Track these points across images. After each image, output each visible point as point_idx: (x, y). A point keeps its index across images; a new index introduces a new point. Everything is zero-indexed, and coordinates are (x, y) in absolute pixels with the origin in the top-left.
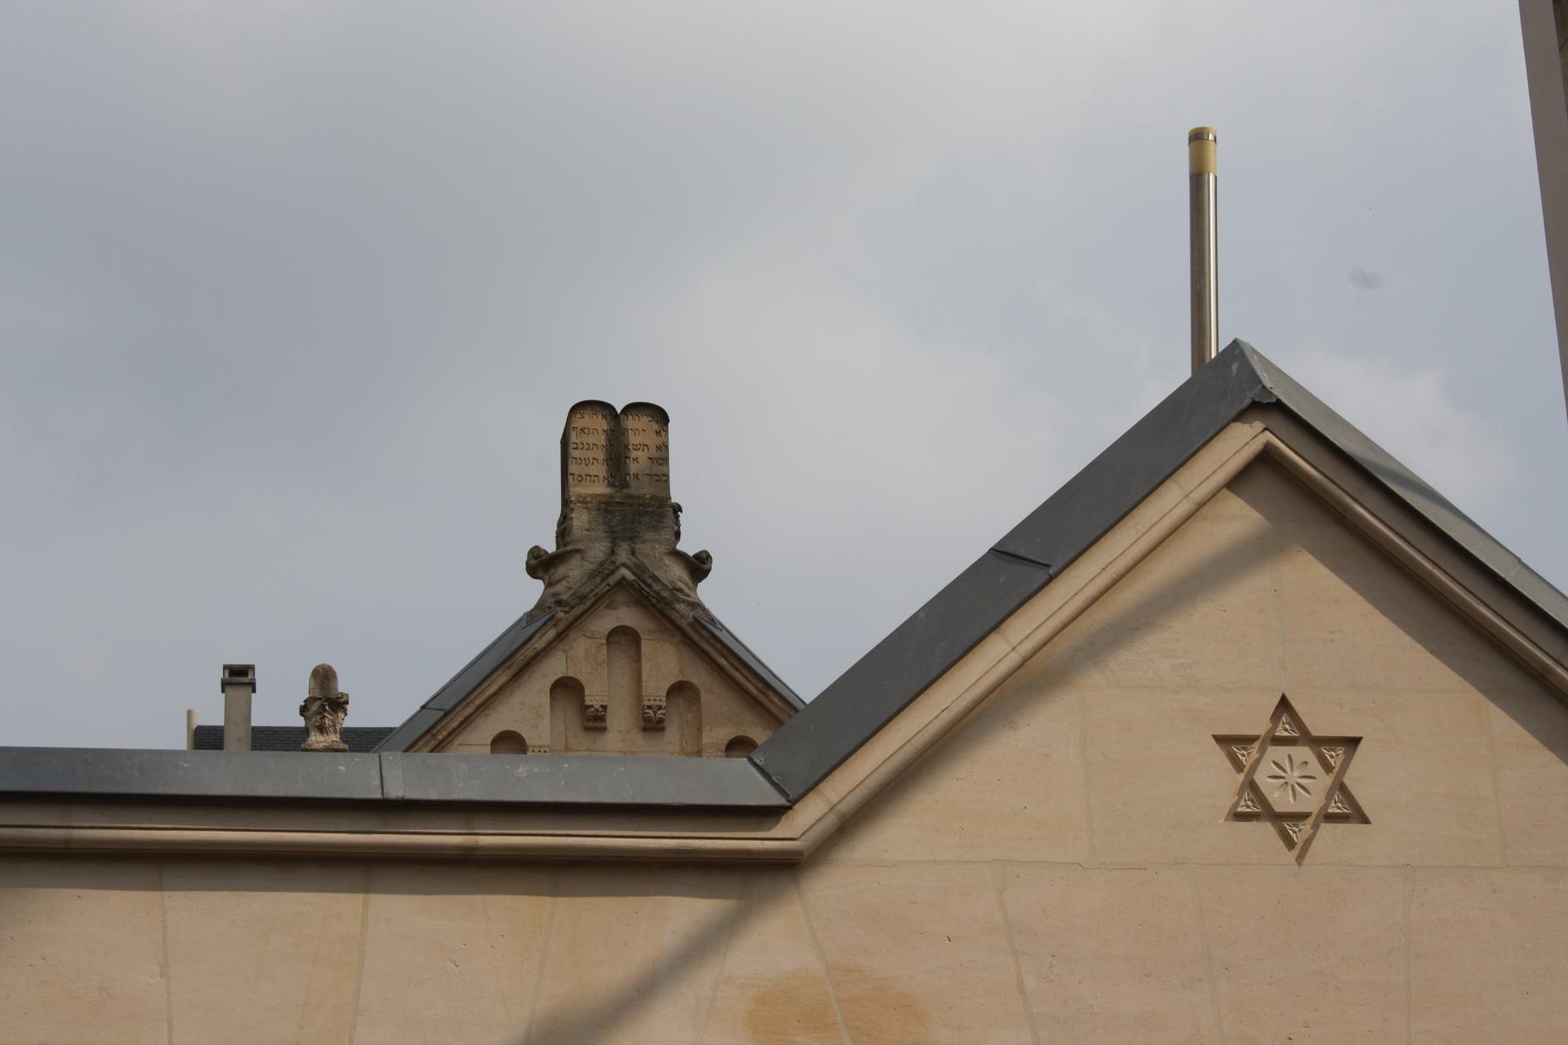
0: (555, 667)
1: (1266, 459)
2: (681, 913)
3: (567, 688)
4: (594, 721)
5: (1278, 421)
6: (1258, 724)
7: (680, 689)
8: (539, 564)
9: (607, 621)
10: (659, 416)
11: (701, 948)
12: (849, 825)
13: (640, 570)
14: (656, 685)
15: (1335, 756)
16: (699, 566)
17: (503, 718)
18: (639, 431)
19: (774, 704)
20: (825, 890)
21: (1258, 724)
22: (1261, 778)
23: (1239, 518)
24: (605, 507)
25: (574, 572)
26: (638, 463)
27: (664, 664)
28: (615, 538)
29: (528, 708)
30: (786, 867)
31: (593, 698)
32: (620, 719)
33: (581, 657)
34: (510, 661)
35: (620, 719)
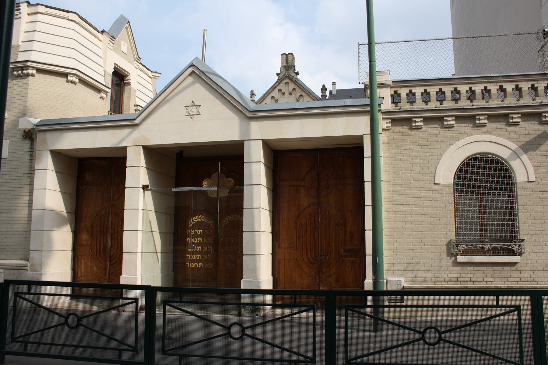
0: (278, 88)
1: (193, 72)
2: (127, 131)
3: (280, 90)
4: (284, 94)
5: (194, 67)
6: (190, 104)
7: (294, 89)
8: (278, 75)
9: (285, 81)
10: (292, 54)
11: (129, 135)
12: (143, 120)
13: (289, 74)
14: (291, 89)
15: (198, 107)
16: (297, 74)
17: (272, 94)
18: (290, 57)
19: (305, 90)
20: (141, 127)
21: (190, 104)
22: (189, 111)
23: (190, 79)
24: (285, 67)
25: (281, 75)
26: (290, 61)
27: (292, 86)
28: (286, 70)
29: (275, 93)
30: (137, 125)
31: (283, 91)
32: (287, 93)
33: (282, 86)
34: (273, 88)
35: (287, 93)
